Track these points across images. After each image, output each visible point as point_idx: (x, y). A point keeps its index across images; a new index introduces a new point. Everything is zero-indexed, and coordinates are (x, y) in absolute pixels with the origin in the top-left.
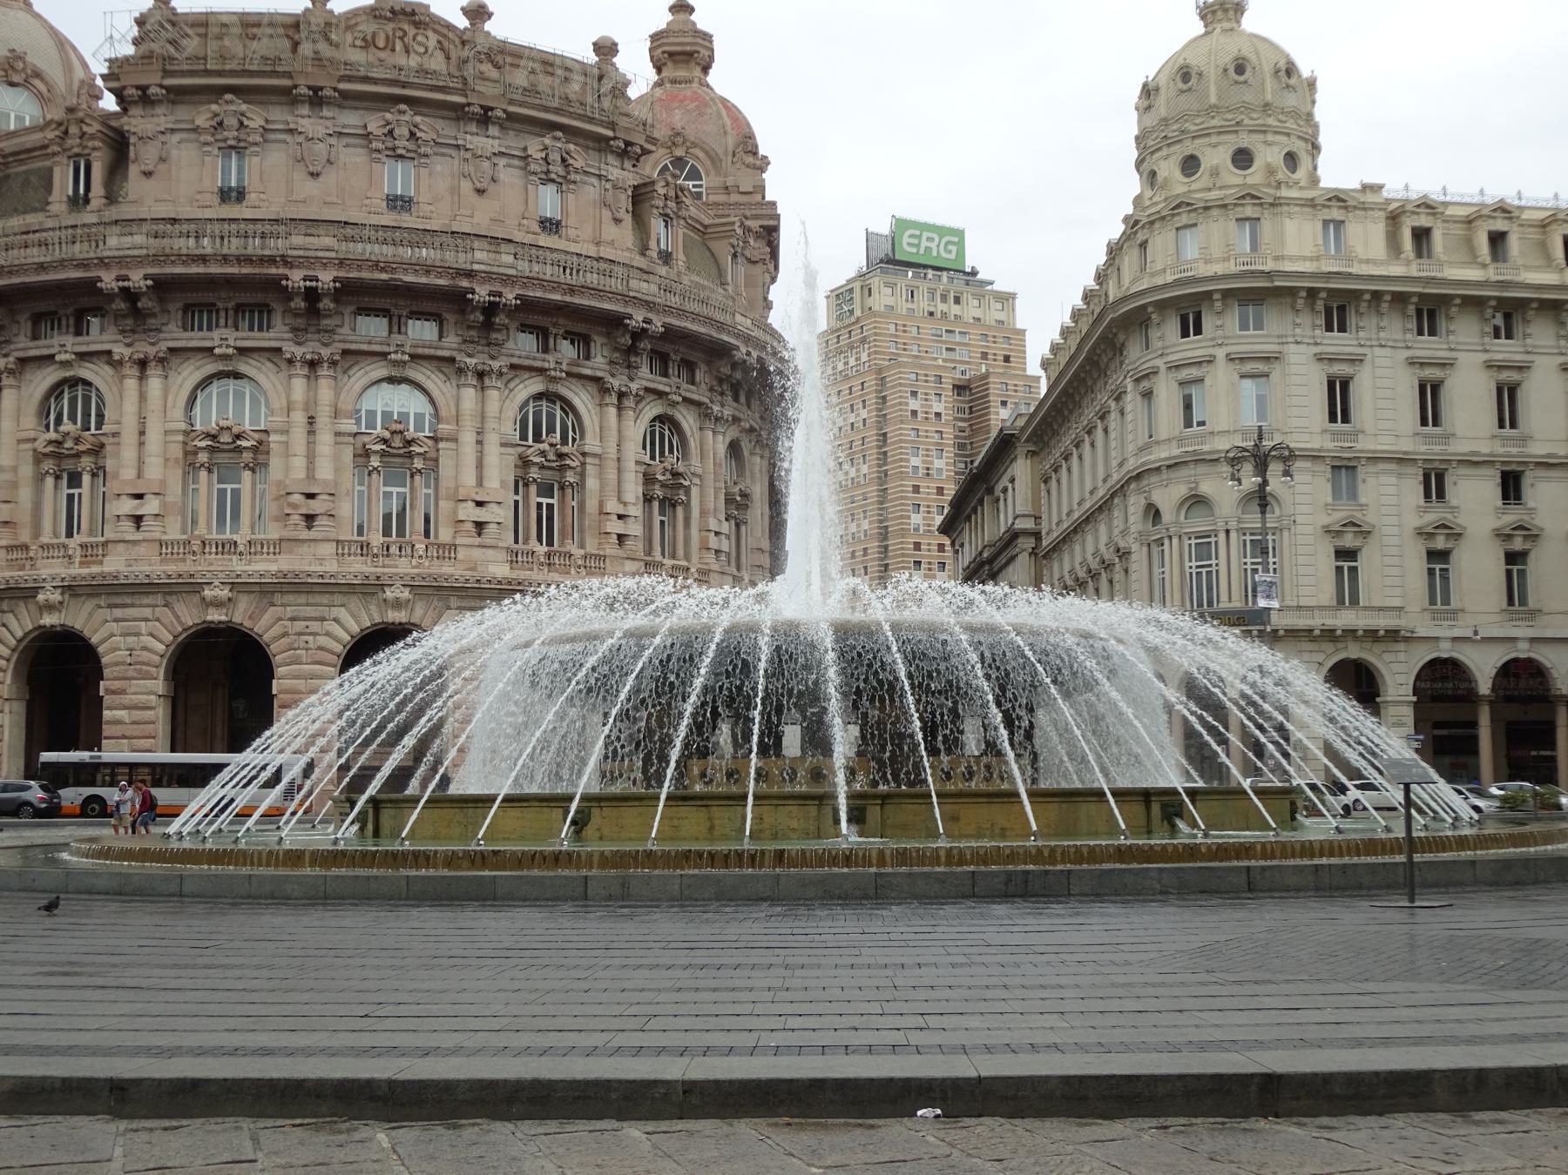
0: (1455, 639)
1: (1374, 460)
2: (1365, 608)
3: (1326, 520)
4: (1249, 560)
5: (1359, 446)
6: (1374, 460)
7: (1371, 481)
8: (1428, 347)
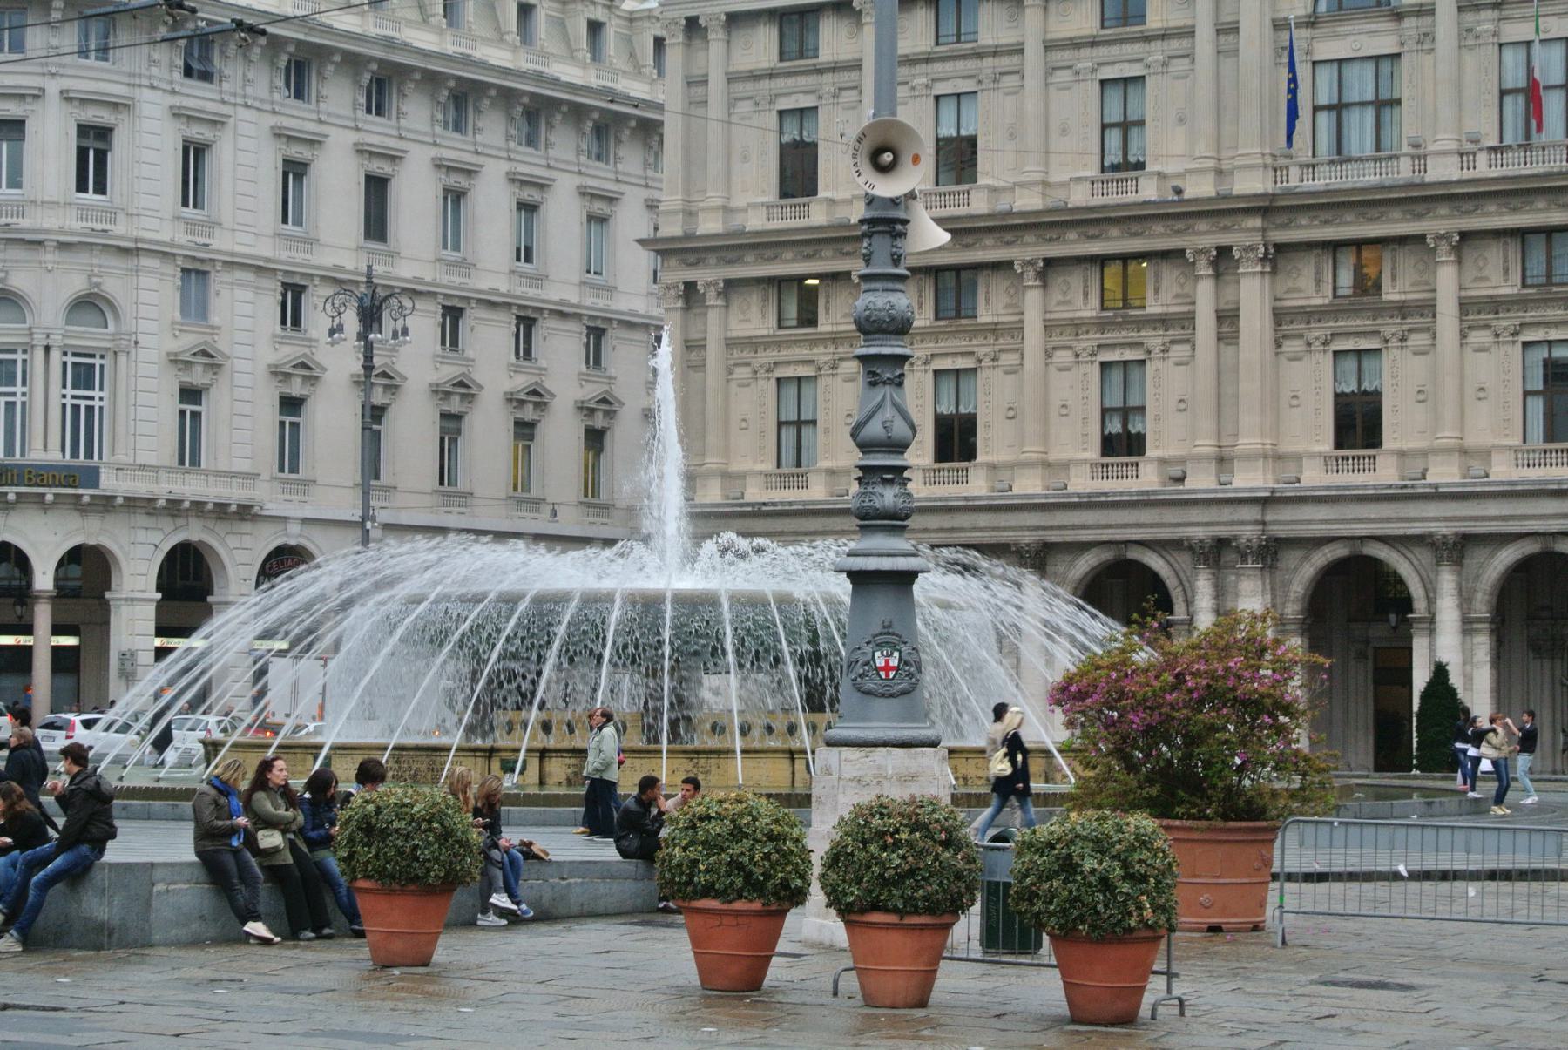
0: (306, 521)
1: (230, 265)
2: (207, 472)
3: (173, 345)
4: (69, 391)
5: (216, 244)
6: (230, 265)
7: (225, 293)
8: (298, 117)
